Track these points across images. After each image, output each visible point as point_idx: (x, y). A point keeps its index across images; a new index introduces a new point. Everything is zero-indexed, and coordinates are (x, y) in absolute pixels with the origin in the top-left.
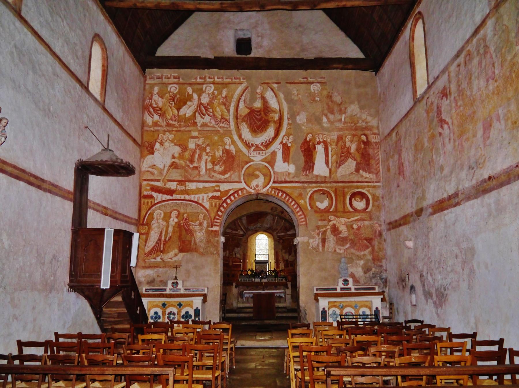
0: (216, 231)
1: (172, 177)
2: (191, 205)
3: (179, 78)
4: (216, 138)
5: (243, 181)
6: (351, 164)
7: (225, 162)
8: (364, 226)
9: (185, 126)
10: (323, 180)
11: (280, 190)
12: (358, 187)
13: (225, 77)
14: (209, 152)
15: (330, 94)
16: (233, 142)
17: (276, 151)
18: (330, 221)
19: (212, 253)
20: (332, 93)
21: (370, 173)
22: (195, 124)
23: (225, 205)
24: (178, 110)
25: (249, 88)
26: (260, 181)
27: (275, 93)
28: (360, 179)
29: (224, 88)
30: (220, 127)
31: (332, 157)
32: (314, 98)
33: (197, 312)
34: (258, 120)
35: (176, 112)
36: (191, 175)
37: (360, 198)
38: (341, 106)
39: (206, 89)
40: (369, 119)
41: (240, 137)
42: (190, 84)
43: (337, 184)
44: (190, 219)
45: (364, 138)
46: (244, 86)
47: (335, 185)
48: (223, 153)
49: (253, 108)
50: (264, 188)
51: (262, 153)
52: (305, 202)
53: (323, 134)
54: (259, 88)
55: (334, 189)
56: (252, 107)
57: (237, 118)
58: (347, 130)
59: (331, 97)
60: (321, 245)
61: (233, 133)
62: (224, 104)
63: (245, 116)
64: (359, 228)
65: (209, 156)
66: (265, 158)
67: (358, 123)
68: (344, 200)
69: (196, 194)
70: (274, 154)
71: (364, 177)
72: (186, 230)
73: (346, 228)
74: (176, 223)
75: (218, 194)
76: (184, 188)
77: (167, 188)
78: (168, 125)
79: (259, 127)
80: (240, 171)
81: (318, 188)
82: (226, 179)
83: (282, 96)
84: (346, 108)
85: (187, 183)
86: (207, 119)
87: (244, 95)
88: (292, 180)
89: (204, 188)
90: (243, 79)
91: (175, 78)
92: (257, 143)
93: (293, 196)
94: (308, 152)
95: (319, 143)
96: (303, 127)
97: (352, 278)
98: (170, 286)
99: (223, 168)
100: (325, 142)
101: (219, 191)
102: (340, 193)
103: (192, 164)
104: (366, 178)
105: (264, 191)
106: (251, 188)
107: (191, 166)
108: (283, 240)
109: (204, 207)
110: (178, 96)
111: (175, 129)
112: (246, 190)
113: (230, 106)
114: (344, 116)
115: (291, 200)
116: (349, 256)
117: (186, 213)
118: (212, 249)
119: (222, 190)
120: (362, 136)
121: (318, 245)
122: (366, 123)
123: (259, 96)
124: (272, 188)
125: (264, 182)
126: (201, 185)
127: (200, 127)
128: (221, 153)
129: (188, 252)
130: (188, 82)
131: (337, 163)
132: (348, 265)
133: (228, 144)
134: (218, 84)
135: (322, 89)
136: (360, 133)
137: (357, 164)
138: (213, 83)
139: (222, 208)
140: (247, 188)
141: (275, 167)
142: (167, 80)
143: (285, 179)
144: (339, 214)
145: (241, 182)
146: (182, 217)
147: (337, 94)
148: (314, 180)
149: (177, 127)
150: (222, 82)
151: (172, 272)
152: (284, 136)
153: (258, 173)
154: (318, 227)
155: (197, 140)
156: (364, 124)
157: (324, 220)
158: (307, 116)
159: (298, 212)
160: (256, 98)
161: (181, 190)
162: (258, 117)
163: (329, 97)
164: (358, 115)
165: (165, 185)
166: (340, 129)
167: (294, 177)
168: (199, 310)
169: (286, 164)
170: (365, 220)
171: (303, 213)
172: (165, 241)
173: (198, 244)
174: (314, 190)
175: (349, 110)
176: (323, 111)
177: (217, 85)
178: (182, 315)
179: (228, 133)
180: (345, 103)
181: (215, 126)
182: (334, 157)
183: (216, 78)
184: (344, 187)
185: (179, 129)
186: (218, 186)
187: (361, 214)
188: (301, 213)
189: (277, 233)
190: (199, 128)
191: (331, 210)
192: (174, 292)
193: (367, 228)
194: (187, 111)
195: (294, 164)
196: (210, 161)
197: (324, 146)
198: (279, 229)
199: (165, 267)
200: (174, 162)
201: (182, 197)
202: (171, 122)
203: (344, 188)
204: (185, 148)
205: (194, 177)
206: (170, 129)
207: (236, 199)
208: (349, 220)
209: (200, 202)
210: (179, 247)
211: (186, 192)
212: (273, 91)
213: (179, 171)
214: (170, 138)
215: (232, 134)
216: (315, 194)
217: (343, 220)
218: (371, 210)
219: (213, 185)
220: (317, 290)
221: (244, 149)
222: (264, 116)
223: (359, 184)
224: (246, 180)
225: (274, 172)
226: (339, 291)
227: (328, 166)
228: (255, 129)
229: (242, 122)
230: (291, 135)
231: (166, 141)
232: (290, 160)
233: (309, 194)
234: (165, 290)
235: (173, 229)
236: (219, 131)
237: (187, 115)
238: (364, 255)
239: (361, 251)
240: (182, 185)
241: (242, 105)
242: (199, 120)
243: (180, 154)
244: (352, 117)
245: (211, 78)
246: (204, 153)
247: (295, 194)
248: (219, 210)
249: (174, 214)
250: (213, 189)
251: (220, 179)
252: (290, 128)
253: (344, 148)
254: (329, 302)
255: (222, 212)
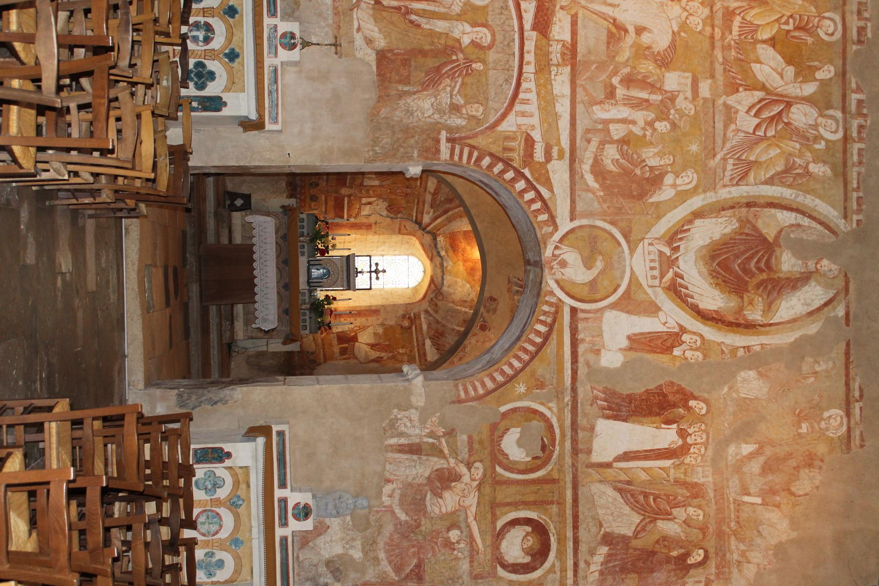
0: (438, 151)
1: (585, 27)
2: (507, 81)
3: (860, 42)
4: (694, 148)
5: (576, 223)
6: (624, 521)
7: (626, 173)
8: (457, 559)
9: (726, 61)
10: (580, 446)
11: (551, 327)
12: (561, 541)
13: (863, 170)
14: (655, 130)
15: (817, 463)
16: (682, 196)
17: (660, 313)
18: (469, 466)
19: (376, 141)
20: (820, 468)
21: (601, 573)
22: (733, 88)
23: (510, 175)
24: (772, 42)
25: (833, 239)
26: (577, 272)
27: (819, 309)
28: (583, 548)
29: (833, 168)
30: (724, 159)
31: (643, 469)
32: (806, 419)
33: (214, 104)
34: (746, 265)
35: (766, 35)
36: (591, 79)
37: (531, 548)
38: (783, 494)
39: (831, 117)
40: (750, 571)
41: (698, 214)
42: (843, 74)
43: (569, 486)
44: (469, 80)
45: (697, 556)
46: (841, 225)
47: (569, 478)
48: (652, 168)
49: (778, 251)
50: (557, 282)
51: (654, 277)
52: (521, 397)
53: (706, 445)
54: (834, 267)
55: (556, 476)
56: (780, 246)
57: (749, 205)
58: (720, 510)
59: (810, 466)
60: (403, 441)
61: (708, 194)
62: (787, 171)
63: (755, 228)
64: (449, 545)
65: (644, 129)
66: (640, 285)
67: (737, 539)
68: (526, 504)
69: (538, 94)
70: (653, 309)
71: (588, 558)
72: (438, 69)
73: (449, 509)
74: (458, 41)
75: (539, 155)
76: (555, 61)
77: (553, 13)
78: (729, 15)
79: (725, 266)
80: (603, 216)
81: (557, 431)
82: (582, 177)
83: (813, 329)
84: (778, 506)
85: (569, 68)
86: (748, 123)
87: (814, 224)
88: (581, 359)
89: (557, 117)
90: (859, 222)
91: (861, 30)
92: (681, 262)
93: (536, 362)
94: (658, 405)
95: (682, 433)
96: (726, 389)
97: (315, 527)
98: (284, 27)
99: (612, 168)
100: (684, 449)
101: (548, 158)
102: (544, 492)
103: (621, 81)
104: (588, 564)
105: (550, 283)
106: (556, 248)
107: (615, 81)
108: (410, 328)
109: (504, 116)
110: (810, 40)
111: (718, 32)
112: (552, 234)
113: (783, 184)
114: (759, 500)
115: (526, 357)
116: (372, 518)
117: (486, 70)
118: (386, 140)
119: (549, 166)
120: (701, 552)
121: (401, 435)
122: (739, 563)
123: (811, 266)
124: (558, 306)
125: (574, 283)
126: (563, 108)
127: (725, 104)
128: (652, 162)
129: (379, 75)
130: (848, 68)
131: (629, 483)
132: (348, 518)
133: (679, 181)
134: (845, 151)
135: (832, 439)
136: (711, 544)
137: (625, 539)
138: (846, 138)
139: (500, 167)
140: (557, 236)
141: (615, 312)
142: (855, 8)
143: (583, 340)
144: (487, 490)
145: (571, 220)
146: (473, 57)
147: (817, 482)
148: (582, 421)
149: (723, 38)
150: (849, 163)
151: (321, 33)
152: (701, 336)
153: (599, 264)
154: (450, 433)
155: (689, 94)
156: (736, 556)
157: (471, 449)
158: (757, 399)
159: (493, 379)
160: (805, 259)
161: (548, 53)
162: (752, 264)
163: (810, 461)
164: (759, 541)
165: (562, 8)
166: (720, 491)
167: (588, 364)
168: (219, 110)
169: (625, 343)
170: (471, 562)
171: (489, 393)
172: (409, 11)
173: (402, 102)
174: (554, 421)
175: (773, 516)
176: (772, 443)
177: (840, 147)
178: (206, 62)
179: (708, 182)
180: (795, 505)
181: (728, 145)
182: (643, 476)
183: (863, 146)
184: (561, 503)
185: (718, 44)
186: (561, 156)
187: (489, 550)
188: (490, 385)
189: (426, 312)
190: (720, 101)
191: (499, 469)
192: (269, 38)
193: (451, 568)
194: (769, 67)
195: (625, 365)
196: (631, 132)
197: (674, 446)
198: (437, 316)
199: (337, 14)
200: (626, 31)
201: (529, 57)
202: (737, 21)
203: (558, 503)
204: (665, 61)
205: (585, 90)
206: (718, 21)
207: (525, 207)
208: (471, 519)
209: (517, 107)
210: (391, 51)
211: (543, 66)
212: (826, 304)
213: (603, 47)
214: (691, 18)
215: (704, 191)
216: (542, 424)
217: (472, 501)
218: (501, 578)
219: (565, 143)
220: (281, 434)
221: (663, 226)
222: (755, 281)
223: (570, 544)
224: (579, 233)
225: (601, 310)
226: (278, 493)
227: (618, 459)
228: (719, 255)
229: (740, 220)
230: (705, 356)
231: (685, 9)
232: (633, 355)
233: (541, 409)
234: (273, 15)
235: (441, 33)
236: (714, 156)
237: (756, 67)
238: (376, 559)
239: (386, 552)
240: (563, 54)
241: (786, 218)
242: (745, 99)
243: (649, 48)
244: (756, 523)
245: (859, 132)
246: (651, 116)
247: (540, 368)
248: (496, 159)
249: (484, 35)
250: (553, 142)
251: (581, 161)
252: (723, 352)
253: (668, 503)
254: (246, 468)
255: (490, 167)
